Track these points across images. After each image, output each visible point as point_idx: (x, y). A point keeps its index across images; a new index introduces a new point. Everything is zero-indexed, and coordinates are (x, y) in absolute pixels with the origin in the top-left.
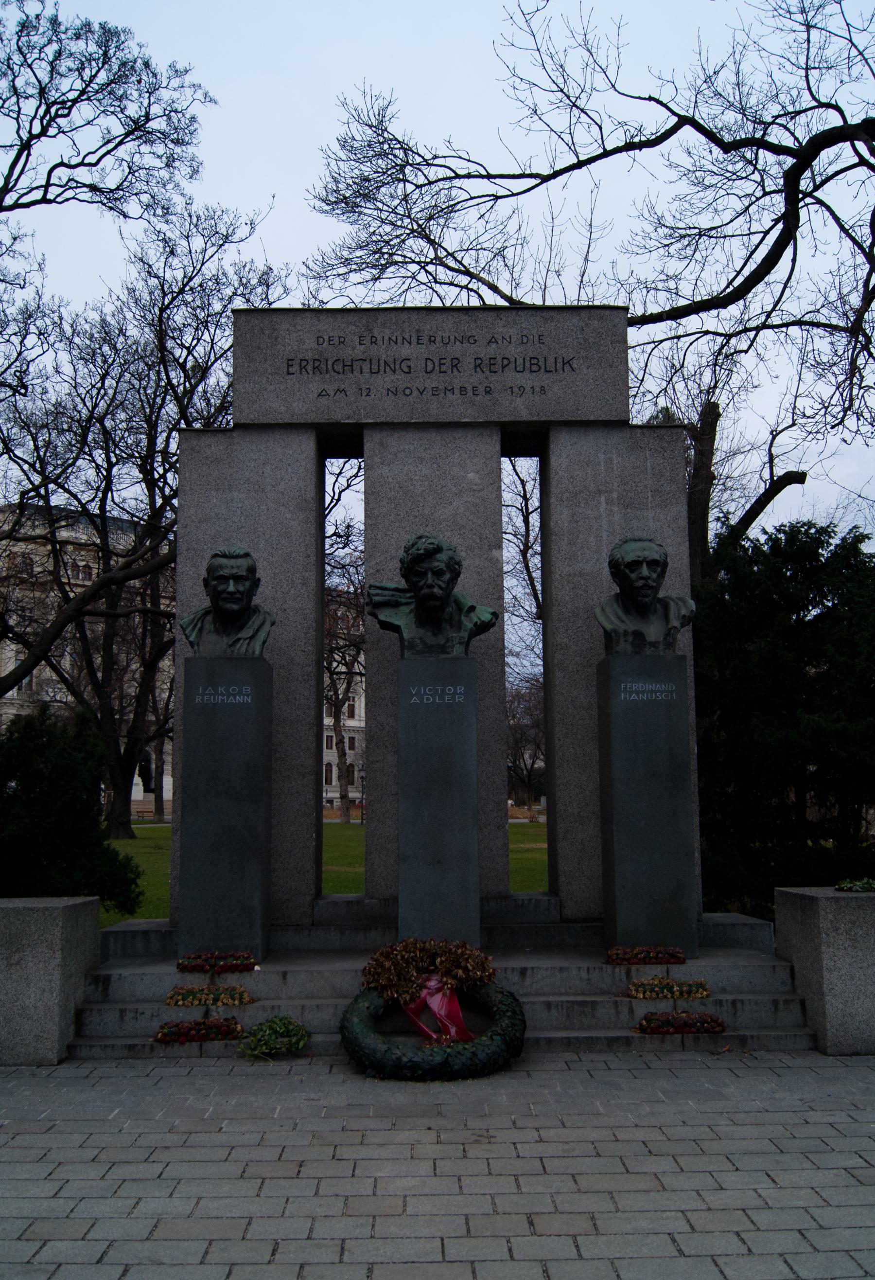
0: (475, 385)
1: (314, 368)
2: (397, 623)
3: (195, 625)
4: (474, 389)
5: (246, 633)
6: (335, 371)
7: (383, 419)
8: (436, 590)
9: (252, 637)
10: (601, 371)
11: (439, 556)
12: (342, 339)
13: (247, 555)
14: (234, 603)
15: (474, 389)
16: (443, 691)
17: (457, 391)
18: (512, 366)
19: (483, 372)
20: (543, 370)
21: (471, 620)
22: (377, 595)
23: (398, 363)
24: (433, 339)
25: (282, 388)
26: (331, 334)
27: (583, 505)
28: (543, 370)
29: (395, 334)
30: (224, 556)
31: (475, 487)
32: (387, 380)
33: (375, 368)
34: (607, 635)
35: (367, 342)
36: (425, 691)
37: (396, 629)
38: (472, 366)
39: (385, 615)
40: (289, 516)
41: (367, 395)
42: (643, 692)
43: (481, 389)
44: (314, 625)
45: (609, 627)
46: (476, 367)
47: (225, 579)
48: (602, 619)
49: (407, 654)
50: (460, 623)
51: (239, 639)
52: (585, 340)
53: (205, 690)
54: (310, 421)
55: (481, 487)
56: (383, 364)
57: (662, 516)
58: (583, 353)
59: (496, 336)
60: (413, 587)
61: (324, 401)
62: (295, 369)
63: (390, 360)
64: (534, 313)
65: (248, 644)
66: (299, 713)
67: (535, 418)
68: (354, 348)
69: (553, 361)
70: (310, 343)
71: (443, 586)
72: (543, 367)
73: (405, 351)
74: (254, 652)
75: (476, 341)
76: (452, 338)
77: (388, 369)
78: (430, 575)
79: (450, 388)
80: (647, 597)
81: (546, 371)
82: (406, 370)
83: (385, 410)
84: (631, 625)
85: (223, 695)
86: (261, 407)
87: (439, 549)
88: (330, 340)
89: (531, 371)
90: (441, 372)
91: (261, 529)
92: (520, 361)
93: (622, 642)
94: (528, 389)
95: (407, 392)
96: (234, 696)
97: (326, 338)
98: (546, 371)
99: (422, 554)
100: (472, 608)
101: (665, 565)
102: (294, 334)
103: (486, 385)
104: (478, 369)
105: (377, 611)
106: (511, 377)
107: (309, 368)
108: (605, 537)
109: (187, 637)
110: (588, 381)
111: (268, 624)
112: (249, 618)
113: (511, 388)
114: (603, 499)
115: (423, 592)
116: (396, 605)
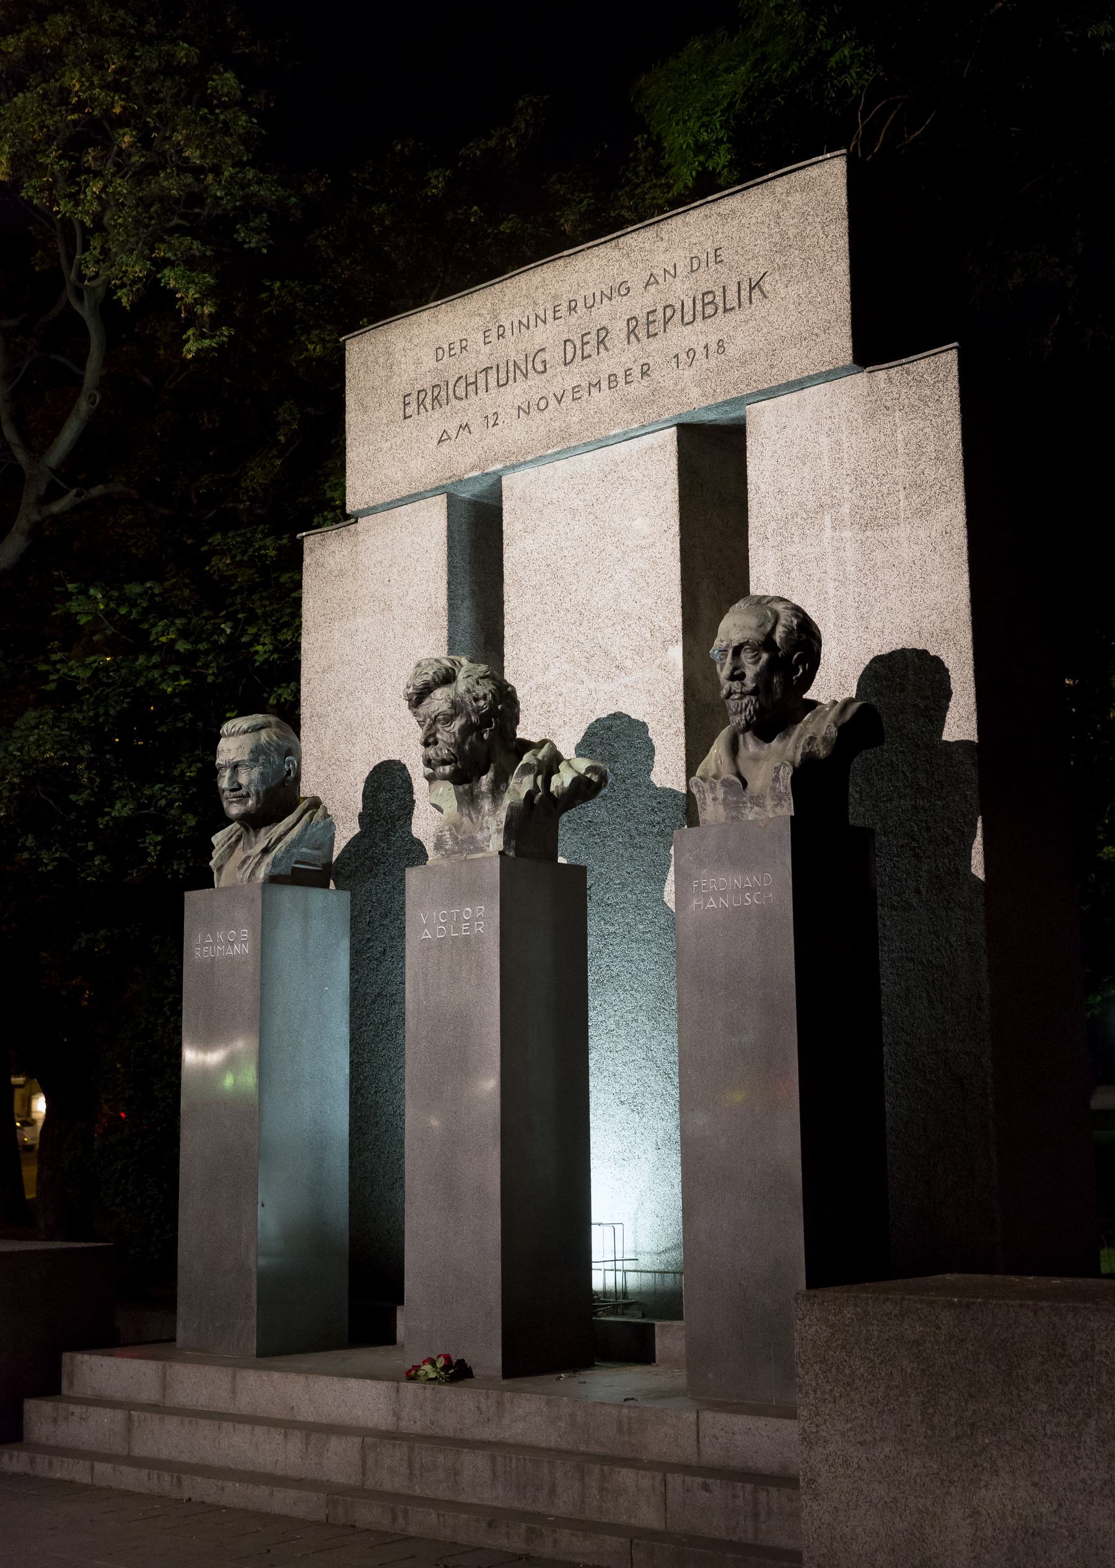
1: (433, 400)
6: (456, 397)
10: (806, 284)
15: (627, 373)
16: (459, 915)
17: (604, 385)
18: (678, 315)
19: (639, 340)
20: (721, 310)
23: (530, 359)
24: (573, 304)
25: (398, 443)
27: (796, 539)
28: (721, 310)
31: (643, 543)
32: (517, 392)
33: (503, 375)
35: (493, 337)
38: (623, 335)
51: (249, 857)
52: (783, 235)
53: (204, 938)
56: (511, 369)
57: (922, 534)
58: (779, 260)
59: (655, 272)
61: (445, 447)
67: (711, 401)
68: (478, 352)
70: (429, 362)
72: (721, 305)
77: (518, 371)
79: (595, 382)
81: (725, 310)
82: (540, 368)
85: (221, 944)
86: (376, 479)
88: (450, 349)
90: (583, 358)
92: (689, 303)
93: (709, 801)
98: (725, 310)
102: (411, 354)
103: (642, 362)
104: (632, 337)
106: (680, 337)
107: (428, 400)
108: (832, 592)
110: (786, 309)
113: (677, 356)
114: (827, 518)
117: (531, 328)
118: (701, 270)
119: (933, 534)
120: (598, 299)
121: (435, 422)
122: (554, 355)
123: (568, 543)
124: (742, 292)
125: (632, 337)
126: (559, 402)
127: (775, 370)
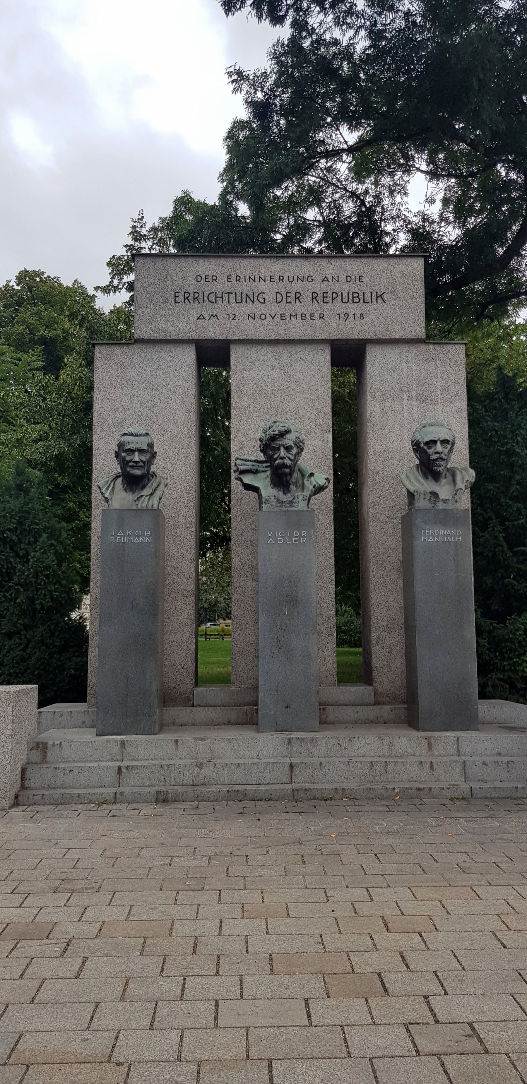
0: (312, 312)
2: (256, 485)
3: (109, 486)
4: (312, 315)
5: (146, 492)
7: (244, 337)
8: (287, 462)
9: (151, 495)
11: (288, 436)
12: (215, 278)
13: (147, 434)
14: (138, 469)
15: (312, 315)
21: (311, 483)
22: (242, 465)
23: (256, 295)
24: (281, 278)
26: (207, 274)
27: (390, 401)
29: (254, 274)
30: (132, 435)
31: (312, 388)
32: (247, 308)
33: (239, 299)
34: (411, 495)
36: (278, 534)
37: (256, 490)
38: (310, 298)
39: (248, 479)
40: (176, 407)
41: (233, 319)
42: (437, 536)
43: (317, 315)
44: (194, 487)
45: (412, 489)
46: (313, 298)
47: (132, 451)
48: (406, 483)
49: (265, 507)
50: (303, 485)
51: (142, 496)
54: (191, 338)
55: (316, 387)
59: (327, 276)
60: (270, 459)
62: (180, 299)
63: (250, 294)
64: (356, 260)
65: (149, 500)
66: (183, 551)
67: (356, 337)
69: (369, 295)
70: (191, 280)
71: (292, 458)
72: (362, 299)
73: (262, 286)
74: (153, 506)
75: (313, 280)
76: (296, 277)
77: (248, 299)
78: (282, 449)
80: (440, 466)
81: (364, 302)
82: (262, 300)
83: (246, 330)
84: (429, 486)
85: (129, 536)
86: (155, 327)
87: (288, 432)
88: (206, 278)
89: (353, 302)
90: (287, 303)
91: (156, 417)
92: (345, 295)
93: (421, 499)
94: (351, 315)
95: (263, 317)
96: (139, 537)
97: (203, 277)
99: (277, 435)
100: (312, 475)
101: (453, 444)
104: (315, 300)
105: (241, 476)
106: (338, 307)
107: (191, 298)
109: (103, 494)
111: (162, 486)
112: (149, 481)
115: (277, 462)
116: (256, 472)
117: (256, 282)
118: (352, 282)
119: (453, 410)
120: (296, 279)
121: (195, 309)
122: (270, 296)
123: (270, 380)
124: (373, 297)
125: (315, 300)
126: (273, 318)
127: (389, 333)
